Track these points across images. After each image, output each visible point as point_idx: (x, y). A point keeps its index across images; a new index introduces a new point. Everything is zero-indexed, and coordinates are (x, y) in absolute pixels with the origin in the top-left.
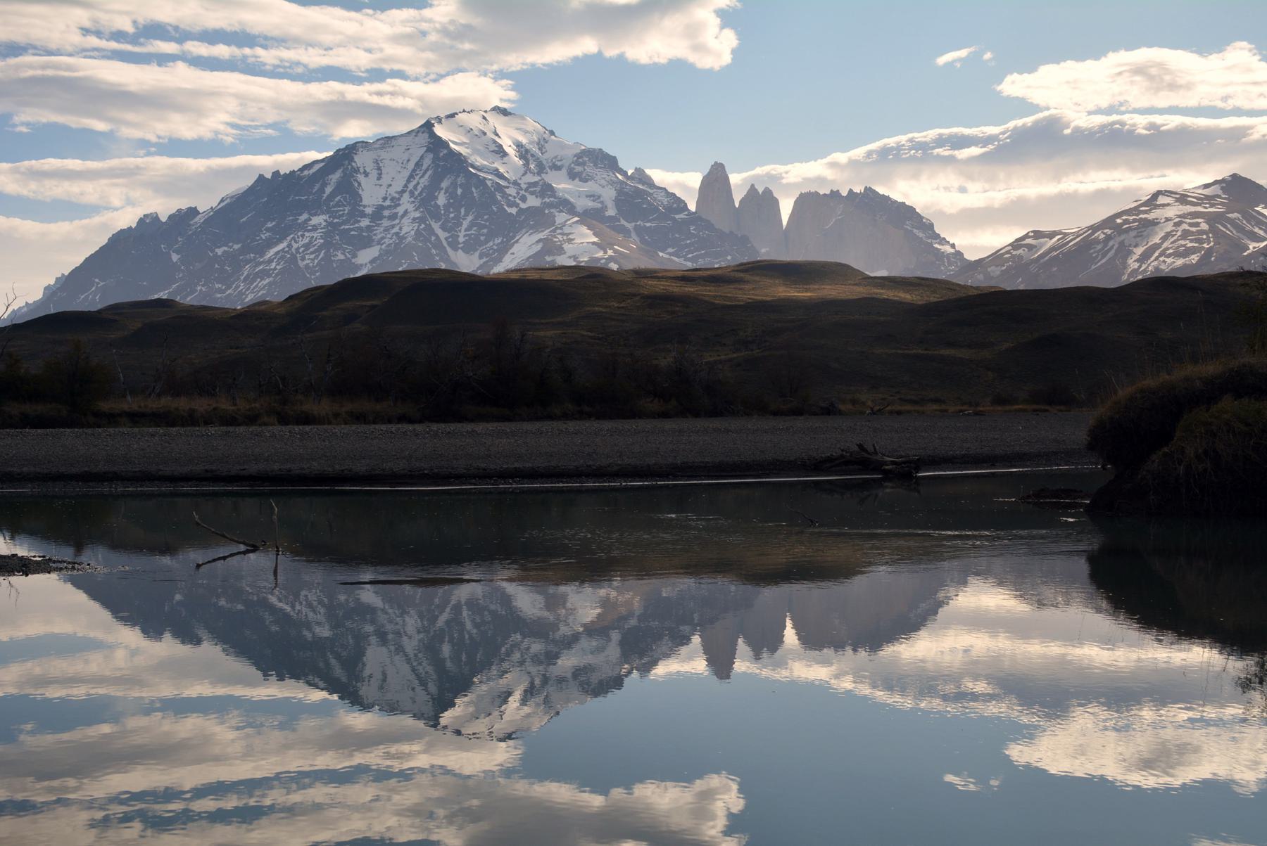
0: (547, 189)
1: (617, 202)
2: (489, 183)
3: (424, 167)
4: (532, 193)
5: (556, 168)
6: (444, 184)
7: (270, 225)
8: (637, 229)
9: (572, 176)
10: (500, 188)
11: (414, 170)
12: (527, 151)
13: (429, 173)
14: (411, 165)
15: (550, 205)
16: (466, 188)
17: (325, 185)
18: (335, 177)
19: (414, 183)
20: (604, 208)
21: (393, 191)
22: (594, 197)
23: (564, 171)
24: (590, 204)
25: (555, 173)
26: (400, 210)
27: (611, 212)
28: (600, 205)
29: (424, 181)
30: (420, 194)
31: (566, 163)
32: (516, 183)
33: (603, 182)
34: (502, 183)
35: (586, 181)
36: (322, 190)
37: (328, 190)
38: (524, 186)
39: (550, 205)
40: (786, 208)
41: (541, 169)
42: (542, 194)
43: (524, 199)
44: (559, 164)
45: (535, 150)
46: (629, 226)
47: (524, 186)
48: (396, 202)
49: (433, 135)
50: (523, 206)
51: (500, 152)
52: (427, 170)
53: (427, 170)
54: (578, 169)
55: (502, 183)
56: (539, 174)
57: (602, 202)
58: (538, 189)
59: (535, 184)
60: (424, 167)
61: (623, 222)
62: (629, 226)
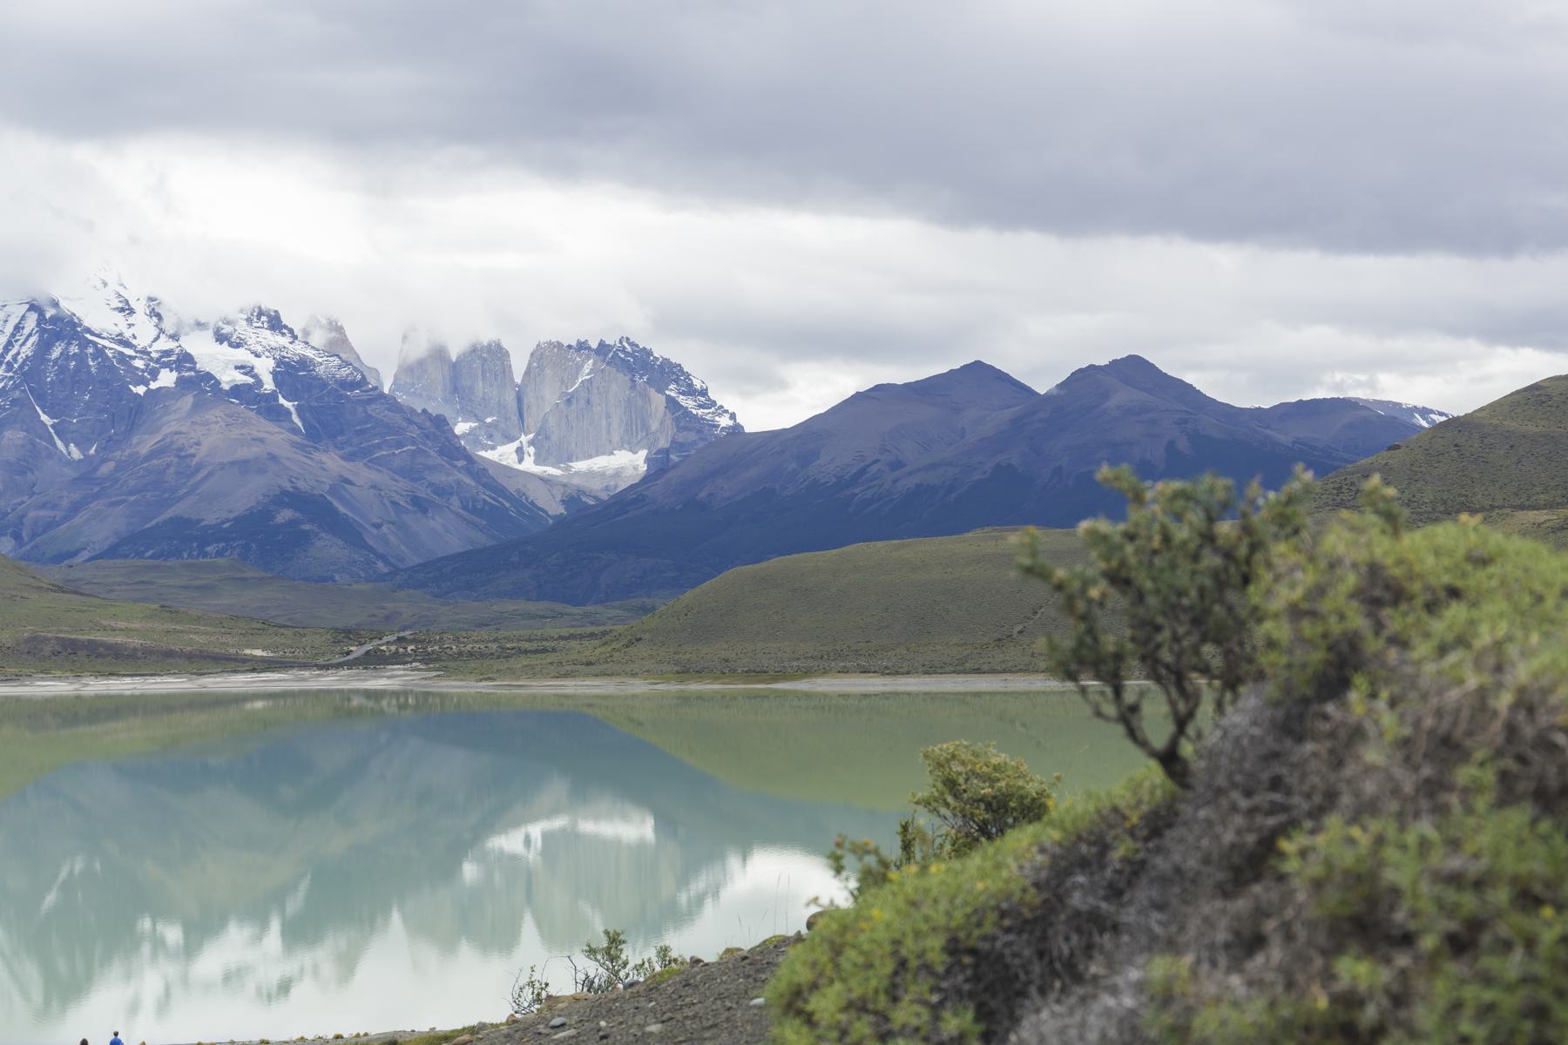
0: (185, 360)
1: (275, 374)
2: (109, 353)
3: (26, 331)
5: (200, 325)
6: (56, 352)
8: (298, 408)
10: (123, 358)
11: (13, 335)
13: (34, 339)
14: (9, 329)
19: (14, 351)
20: (259, 383)
22: (247, 369)
23: (210, 333)
24: (241, 378)
27: (269, 385)
28: (251, 380)
30: (21, 367)
32: (144, 352)
33: (259, 349)
34: (128, 352)
35: (238, 346)
40: (518, 366)
43: (154, 374)
50: (153, 386)
51: (126, 309)
52: (30, 335)
53: (30, 335)
54: (227, 329)
55: (128, 352)
57: (255, 376)
59: (167, 353)
60: (26, 331)
61: (282, 401)
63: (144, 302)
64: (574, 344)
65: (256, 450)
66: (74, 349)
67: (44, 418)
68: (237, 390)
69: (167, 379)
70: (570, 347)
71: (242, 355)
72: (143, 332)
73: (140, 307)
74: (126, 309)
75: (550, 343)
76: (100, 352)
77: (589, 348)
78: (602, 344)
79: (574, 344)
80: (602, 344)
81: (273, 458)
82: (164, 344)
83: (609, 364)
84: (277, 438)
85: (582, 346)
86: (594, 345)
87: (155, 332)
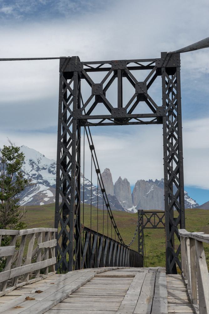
0: (40, 177)
4: (33, 178)
5: (44, 169)
12: (33, 162)
15: (40, 183)
23: (47, 170)
25: (43, 171)
31: (48, 168)
38: (31, 175)
39: (40, 183)
41: (38, 169)
44: (45, 167)
45: (36, 162)
47: (31, 175)
56: (37, 171)
58: (36, 176)
63: (28, 161)
64: (148, 180)
70: (147, 181)
75: (141, 180)
77: (152, 182)
78: (156, 180)
79: (148, 180)
80: (156, 180)
82: (34, 172)
83: (158, 186)
85: (151, 181)
86: (154, 181)
87: (32, 169)
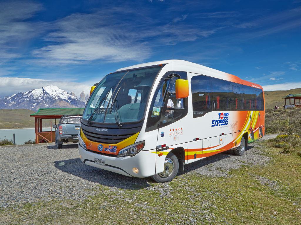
5: (60, 93)
6: (45, 95)
7: (20, 100)
9: (62, 94)
10: (52, 96)
16: (48, 96)
17: (28, 95)
18: (30, 94)
20: (66, 99)
21: (38, 96)
26: (39, 99)
27: (67, 99)
29: (42, 95)
36: (28, 96)
37: (29, 96)
42: (58, 97)
43: (55, 98)
45: (57, 90)
46: (69, 101)
48: (38, 98)
49: (43, 89)
62: (69, 101)
65: (66, 105)
66: (47, 95)
67: (44, 102)
68: (64, 99)
69: (57, 98)
71: (64, 96)
72: (54, 94)
73: (54, 91)
74: (53, 91)
76: (50, 96)
81: (67, 106)
82: (57, 95)
84: (68, 104)
